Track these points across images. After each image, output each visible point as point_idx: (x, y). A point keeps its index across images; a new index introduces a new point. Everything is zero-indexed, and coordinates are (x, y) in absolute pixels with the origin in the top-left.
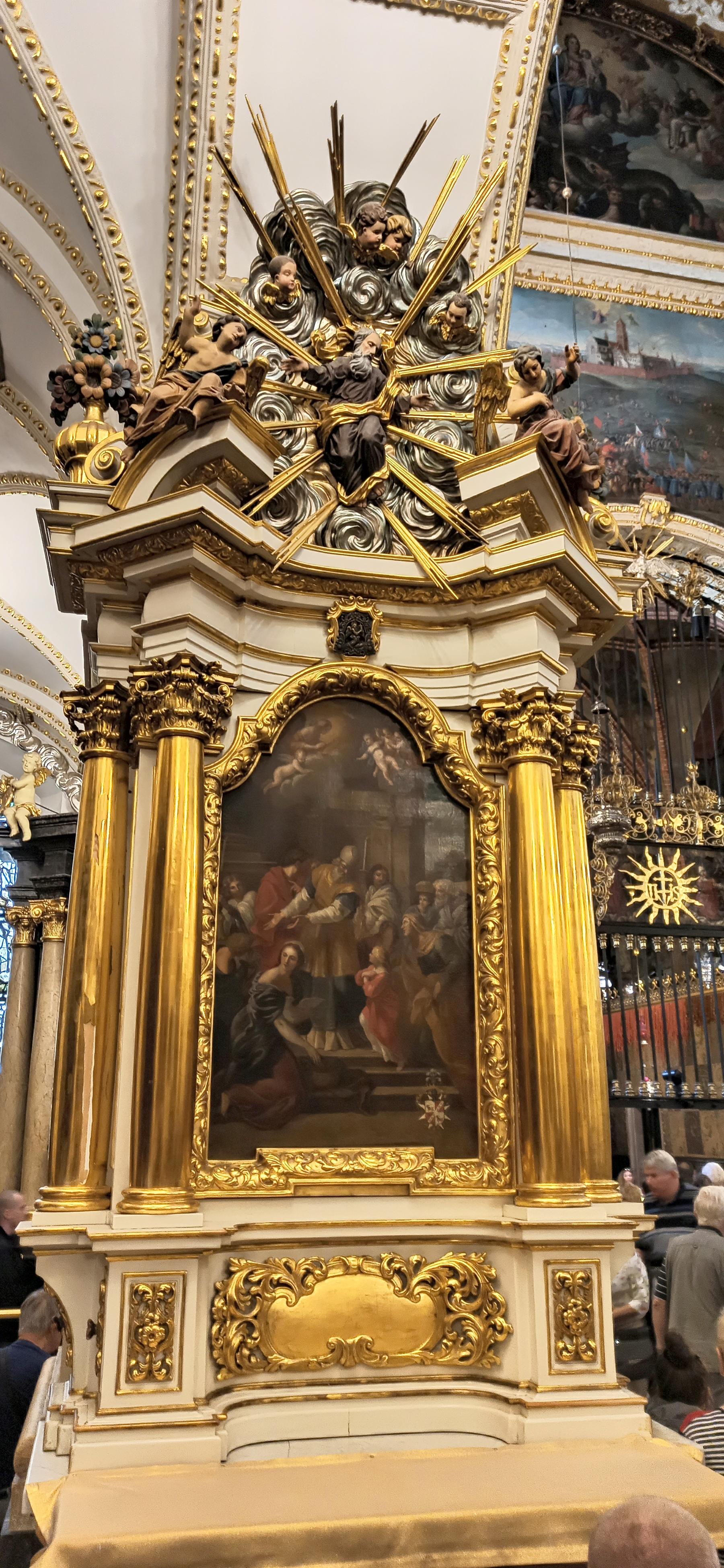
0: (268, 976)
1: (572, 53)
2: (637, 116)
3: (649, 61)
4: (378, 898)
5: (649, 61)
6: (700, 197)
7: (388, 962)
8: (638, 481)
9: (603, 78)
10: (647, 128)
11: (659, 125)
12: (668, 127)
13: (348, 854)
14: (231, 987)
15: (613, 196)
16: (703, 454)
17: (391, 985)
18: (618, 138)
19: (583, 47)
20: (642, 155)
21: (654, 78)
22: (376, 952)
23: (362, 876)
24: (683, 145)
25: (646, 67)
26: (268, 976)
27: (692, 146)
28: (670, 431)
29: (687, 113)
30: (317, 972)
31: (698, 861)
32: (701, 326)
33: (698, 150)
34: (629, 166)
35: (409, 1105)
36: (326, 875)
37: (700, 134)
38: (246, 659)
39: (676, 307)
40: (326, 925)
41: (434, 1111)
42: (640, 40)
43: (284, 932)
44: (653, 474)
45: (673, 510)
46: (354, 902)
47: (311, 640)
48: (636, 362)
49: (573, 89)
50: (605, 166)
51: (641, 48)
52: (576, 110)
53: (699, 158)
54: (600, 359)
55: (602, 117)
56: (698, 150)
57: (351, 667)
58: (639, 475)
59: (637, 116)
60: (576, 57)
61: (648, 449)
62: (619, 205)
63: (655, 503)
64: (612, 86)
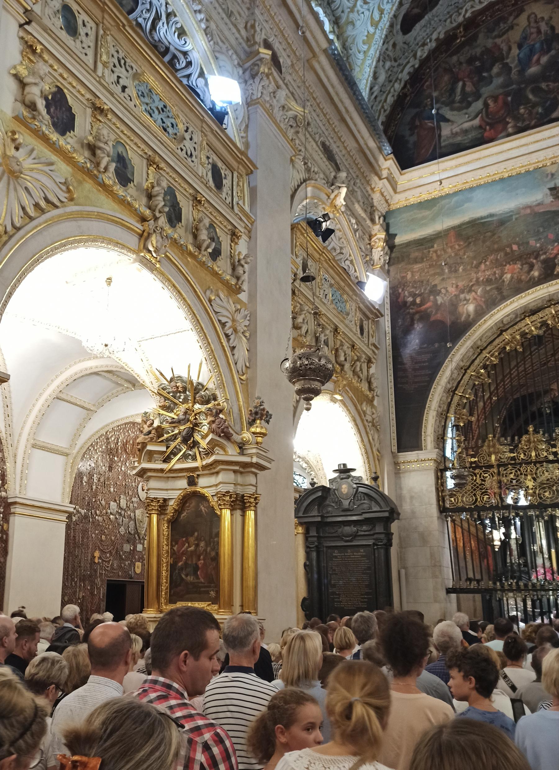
0: (180, 564)
1: (532, 24)
4: (202, 544)
7: (204, 559)
9: (553, 28)
13: (196, 534)
14: (173, 567)
17: (205, 564)
19: (539, 16)
22: (202, 557)
23: (198, 539)
26: (180, 564)
30: (190, 562)
35: (208, 592)
36: (192, 539)
38: (169, 492)
40: (191, 552)
41: (213, 594)
43: (183, 554)
46: (197, 545)
47: (183, 483)
49: (533, 45)
50: (554, 82)
52: (535, 58)
54: (552, 199)
55: (553, 52)
57: (193, 489)
60: (535, 25)
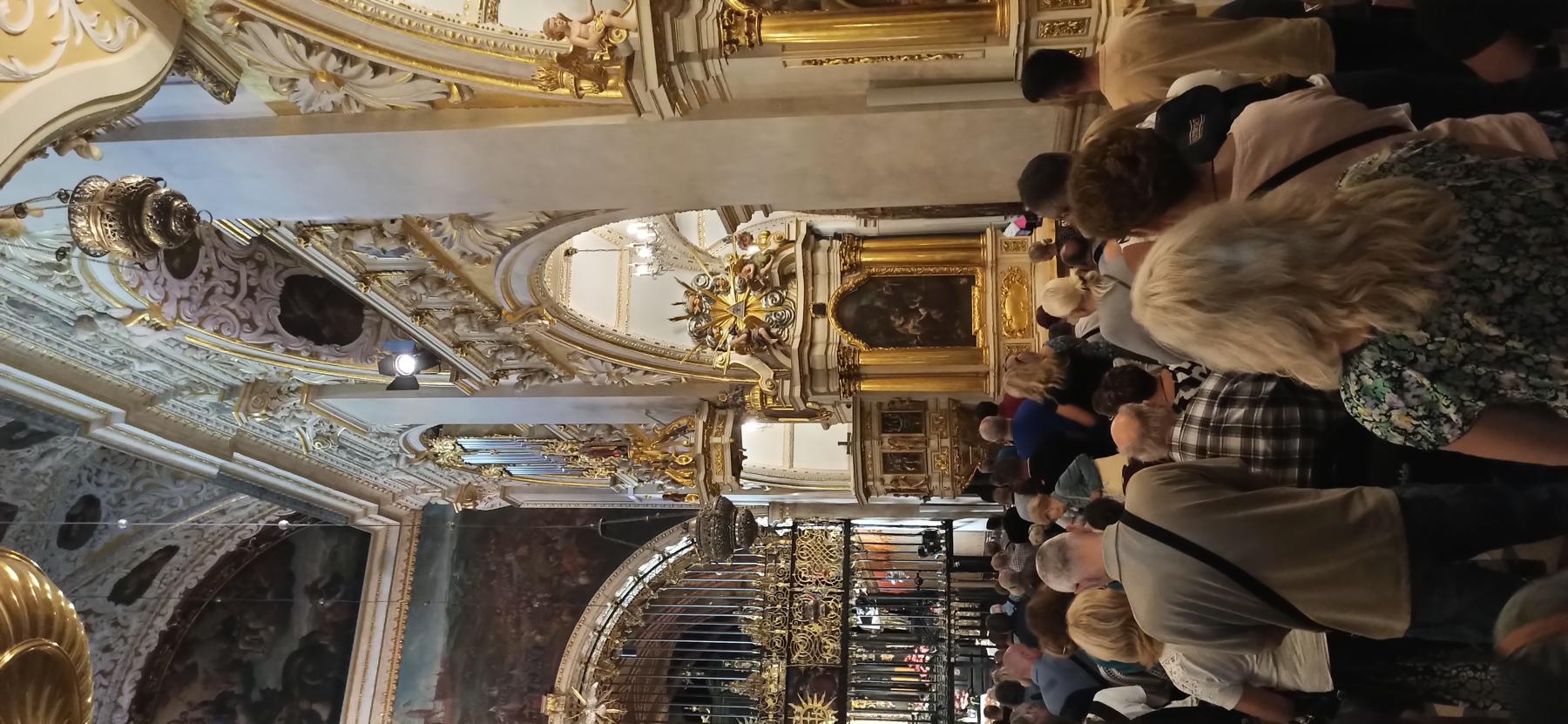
2: (236, 677)
3: (189, 662)
5: (189, 662)
6: (305, 633)
8: (531, 714)
9: (205, 703)
10: (247, 671)
11: (245, 659)
12: (245, 652)
15: (304, 705)
16: (510, 659)
18: (256, 696)
20: (270, 678)
21: (203, 660)
24: (261, 641)
25: (195, 665)
27: (262, 634)
28: (492, 683)
29: (235, 634)
31: (797, 690)
32: (412, 648)
33: (265, 629)
34: (280, 688)
37: (251, 625)
39: (396, 666)
42: (171, 668)
44: (526, 702)
45: (552, 690)
48: (440, 705)
51: (179, 668)
53: (272, 629)
55: (238, 708)
56: (265, 629)
58: (526, 712)
59: (236, 677)
61: (507, 702)
62: (312, 701)
63: (549, 704)
64: (211, 695)
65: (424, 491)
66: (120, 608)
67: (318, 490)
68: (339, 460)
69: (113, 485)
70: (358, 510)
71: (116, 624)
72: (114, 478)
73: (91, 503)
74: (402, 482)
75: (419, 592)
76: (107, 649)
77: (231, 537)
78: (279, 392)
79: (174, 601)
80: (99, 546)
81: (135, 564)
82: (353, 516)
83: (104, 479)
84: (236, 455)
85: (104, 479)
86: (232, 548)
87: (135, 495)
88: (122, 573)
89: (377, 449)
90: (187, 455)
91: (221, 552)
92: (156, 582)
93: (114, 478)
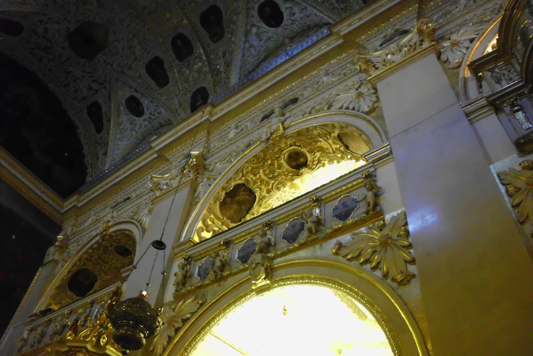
65: (72, 230)
66: (89, 103)
67: (107, 184)
68: (119, 197)
69: (141, 124)
70: (82, 198)
71: (84, 98)
72: (143, 126)
73: (140, 114)
74: (84, 222)
75: (26, 204)
76: (76, 91)
77: (90, 153)
78: (198, 173)
79: (77, 122)
80: (122, 108)
81: (104, 115)
82: (81, 194)
83: (146, 123)
84: (156, 155)
85: (146, 123)
86: (84, 151)
87: (131, 130)
88: (104, 110)
89: (119, 213)
90: (170, 137)
91: (86, 147)
92: (89, 120)
93: (143, 126)
